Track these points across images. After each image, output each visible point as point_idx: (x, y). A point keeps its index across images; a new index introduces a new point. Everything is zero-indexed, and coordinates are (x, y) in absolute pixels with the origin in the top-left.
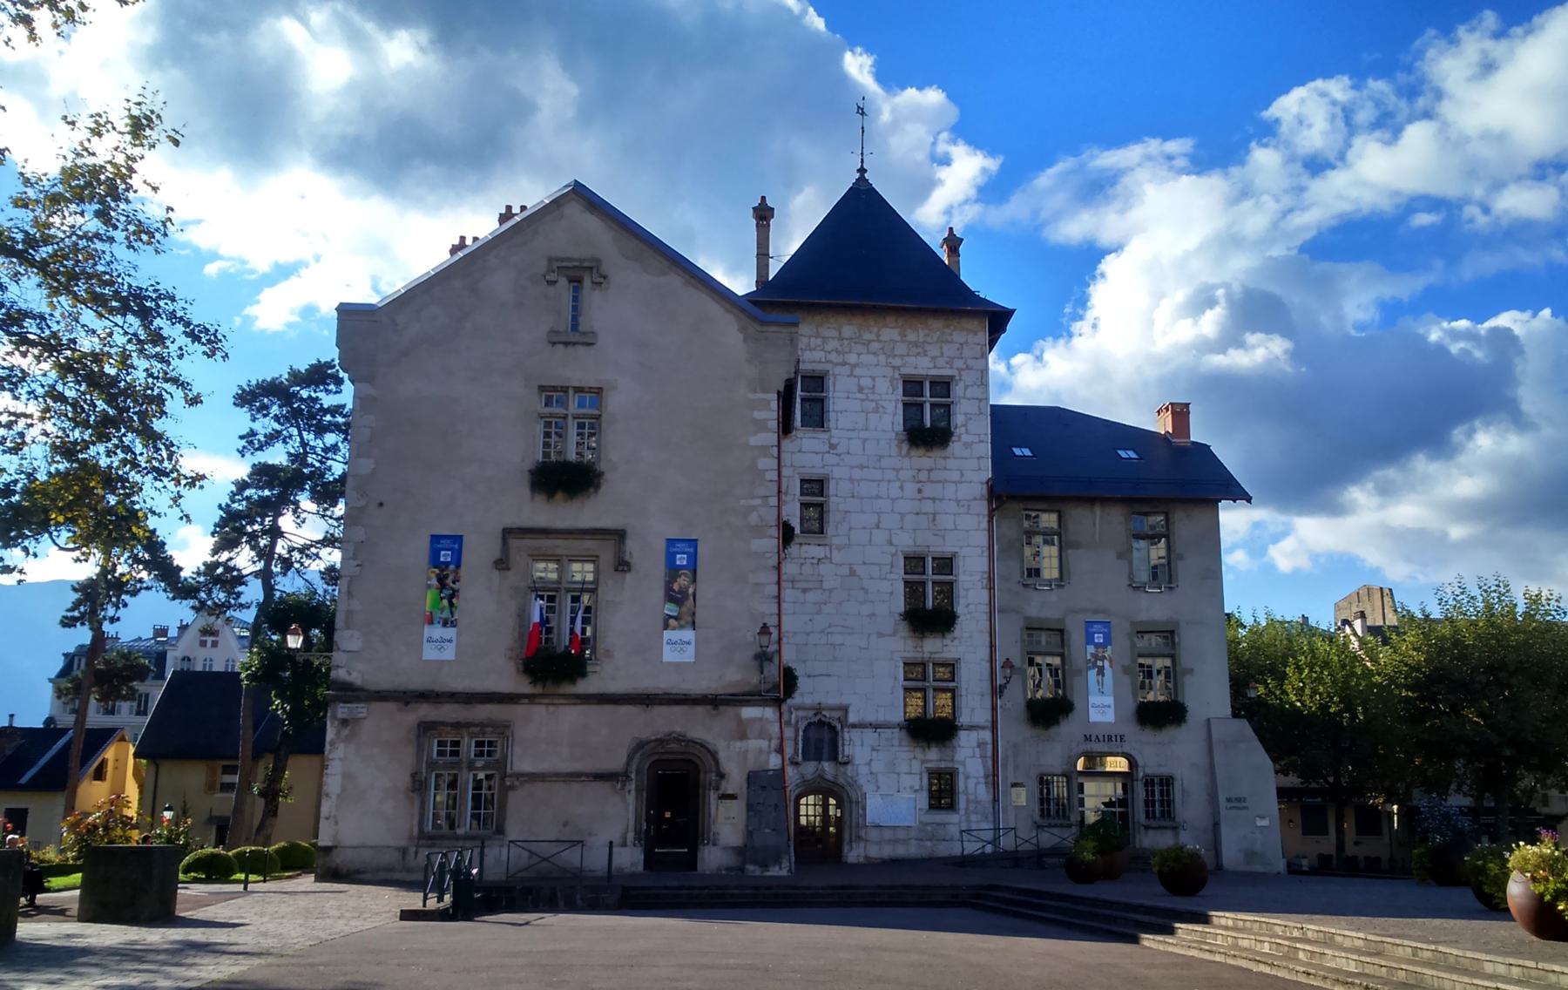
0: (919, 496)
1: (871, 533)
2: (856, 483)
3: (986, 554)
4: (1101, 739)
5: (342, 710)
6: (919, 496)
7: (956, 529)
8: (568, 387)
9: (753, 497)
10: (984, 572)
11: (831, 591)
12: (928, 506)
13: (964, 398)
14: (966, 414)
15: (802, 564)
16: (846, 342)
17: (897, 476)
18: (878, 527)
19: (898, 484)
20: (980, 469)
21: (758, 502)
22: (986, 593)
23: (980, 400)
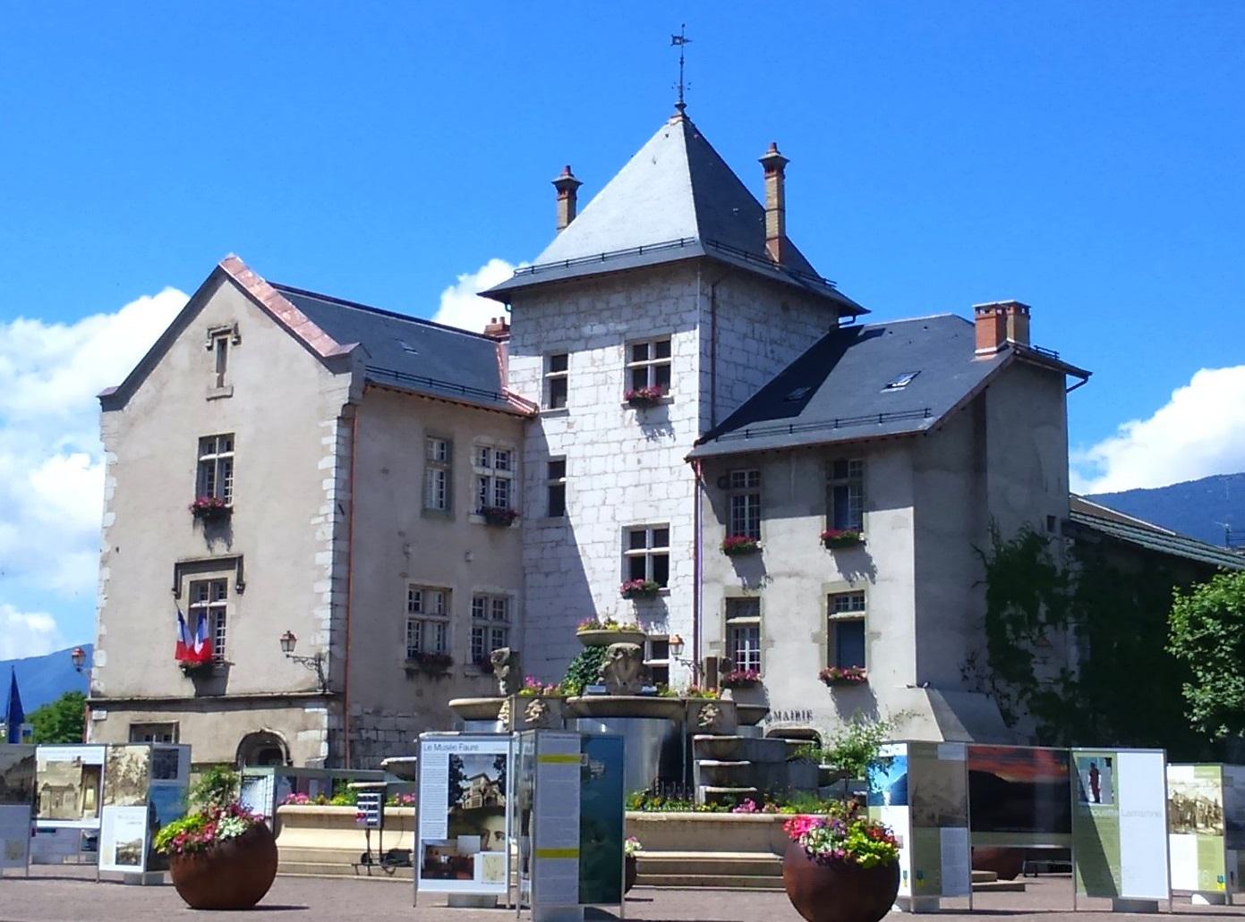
0: (639, 467)
1: (599, 510)
2: (588, 460)
3: (693, 521)
4: (789, 715)
5: (95, 714)
6: (639, 467)
7: (668, 498)
8: (213, 438)
9: (319, 516)
10: (691, 542)
11: (566, 572)
12: (646, 476)
13: (678, 356)
14: (679, 373)
15: (544, 549)
16: (582, 315)
17: (621, 448)
18: (604, 503)
19: (622, 456)
20: (690, 431)
21: (322, 519)
22: (692, 562)
23: (692, 356)
